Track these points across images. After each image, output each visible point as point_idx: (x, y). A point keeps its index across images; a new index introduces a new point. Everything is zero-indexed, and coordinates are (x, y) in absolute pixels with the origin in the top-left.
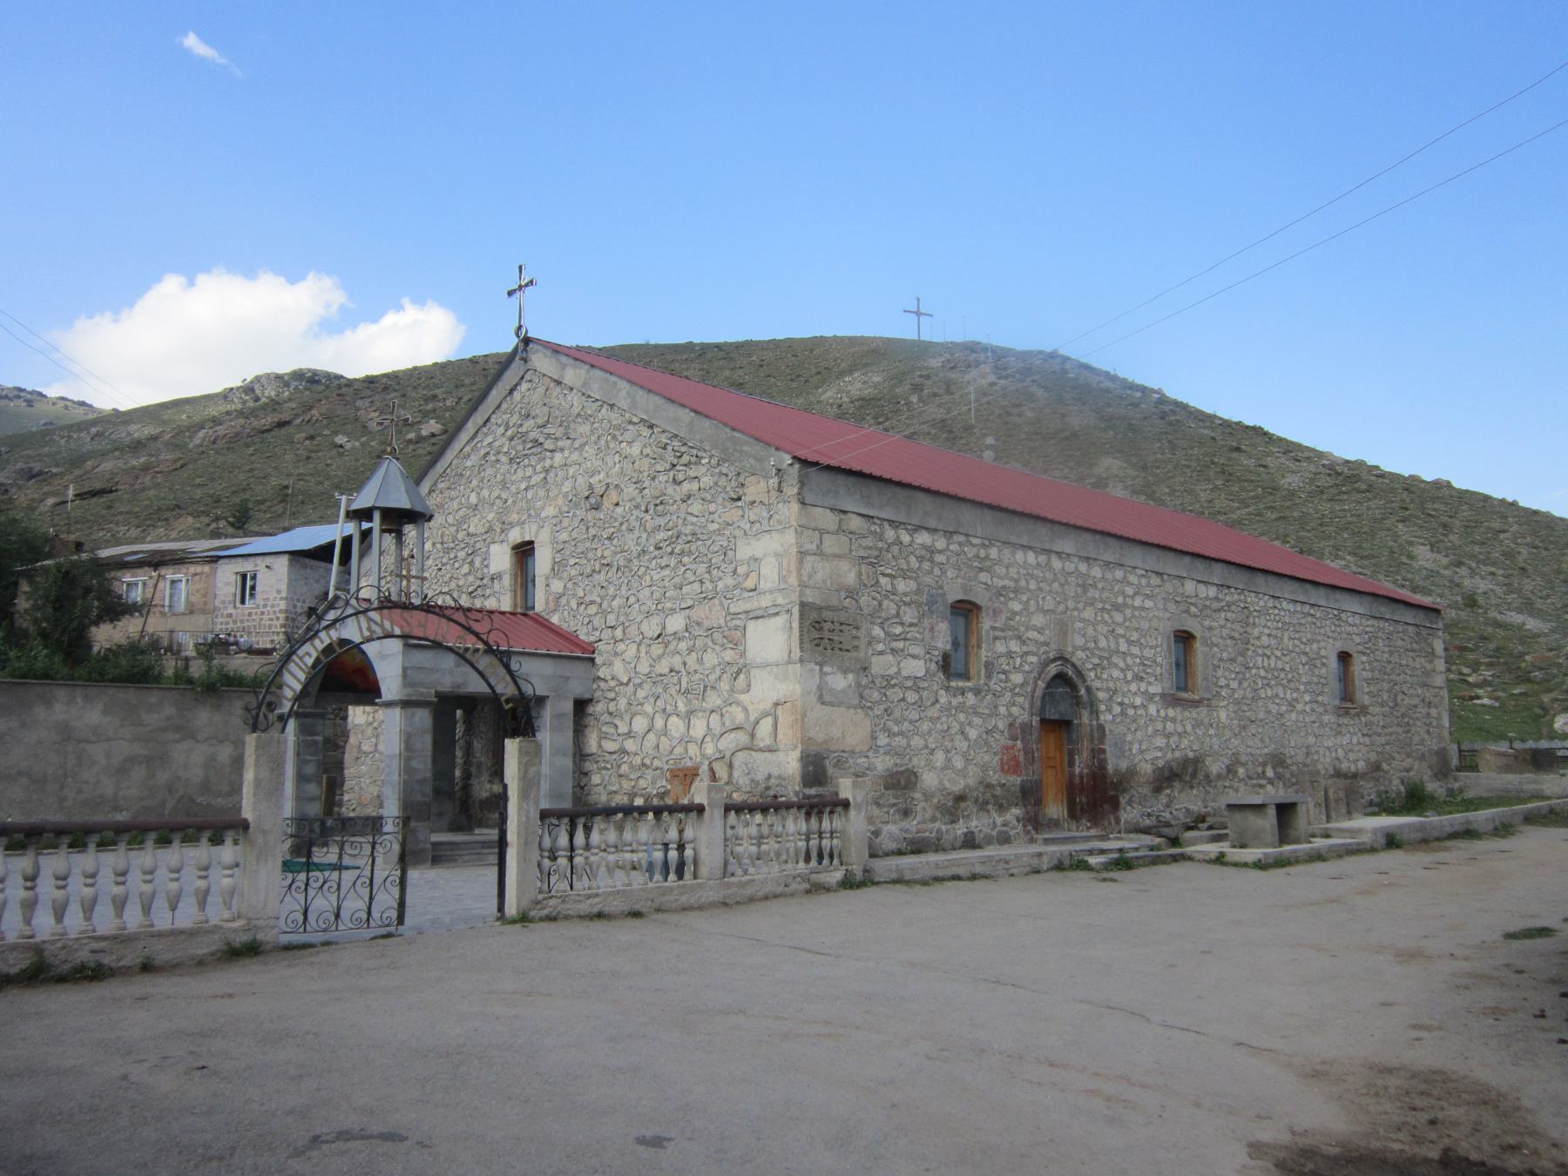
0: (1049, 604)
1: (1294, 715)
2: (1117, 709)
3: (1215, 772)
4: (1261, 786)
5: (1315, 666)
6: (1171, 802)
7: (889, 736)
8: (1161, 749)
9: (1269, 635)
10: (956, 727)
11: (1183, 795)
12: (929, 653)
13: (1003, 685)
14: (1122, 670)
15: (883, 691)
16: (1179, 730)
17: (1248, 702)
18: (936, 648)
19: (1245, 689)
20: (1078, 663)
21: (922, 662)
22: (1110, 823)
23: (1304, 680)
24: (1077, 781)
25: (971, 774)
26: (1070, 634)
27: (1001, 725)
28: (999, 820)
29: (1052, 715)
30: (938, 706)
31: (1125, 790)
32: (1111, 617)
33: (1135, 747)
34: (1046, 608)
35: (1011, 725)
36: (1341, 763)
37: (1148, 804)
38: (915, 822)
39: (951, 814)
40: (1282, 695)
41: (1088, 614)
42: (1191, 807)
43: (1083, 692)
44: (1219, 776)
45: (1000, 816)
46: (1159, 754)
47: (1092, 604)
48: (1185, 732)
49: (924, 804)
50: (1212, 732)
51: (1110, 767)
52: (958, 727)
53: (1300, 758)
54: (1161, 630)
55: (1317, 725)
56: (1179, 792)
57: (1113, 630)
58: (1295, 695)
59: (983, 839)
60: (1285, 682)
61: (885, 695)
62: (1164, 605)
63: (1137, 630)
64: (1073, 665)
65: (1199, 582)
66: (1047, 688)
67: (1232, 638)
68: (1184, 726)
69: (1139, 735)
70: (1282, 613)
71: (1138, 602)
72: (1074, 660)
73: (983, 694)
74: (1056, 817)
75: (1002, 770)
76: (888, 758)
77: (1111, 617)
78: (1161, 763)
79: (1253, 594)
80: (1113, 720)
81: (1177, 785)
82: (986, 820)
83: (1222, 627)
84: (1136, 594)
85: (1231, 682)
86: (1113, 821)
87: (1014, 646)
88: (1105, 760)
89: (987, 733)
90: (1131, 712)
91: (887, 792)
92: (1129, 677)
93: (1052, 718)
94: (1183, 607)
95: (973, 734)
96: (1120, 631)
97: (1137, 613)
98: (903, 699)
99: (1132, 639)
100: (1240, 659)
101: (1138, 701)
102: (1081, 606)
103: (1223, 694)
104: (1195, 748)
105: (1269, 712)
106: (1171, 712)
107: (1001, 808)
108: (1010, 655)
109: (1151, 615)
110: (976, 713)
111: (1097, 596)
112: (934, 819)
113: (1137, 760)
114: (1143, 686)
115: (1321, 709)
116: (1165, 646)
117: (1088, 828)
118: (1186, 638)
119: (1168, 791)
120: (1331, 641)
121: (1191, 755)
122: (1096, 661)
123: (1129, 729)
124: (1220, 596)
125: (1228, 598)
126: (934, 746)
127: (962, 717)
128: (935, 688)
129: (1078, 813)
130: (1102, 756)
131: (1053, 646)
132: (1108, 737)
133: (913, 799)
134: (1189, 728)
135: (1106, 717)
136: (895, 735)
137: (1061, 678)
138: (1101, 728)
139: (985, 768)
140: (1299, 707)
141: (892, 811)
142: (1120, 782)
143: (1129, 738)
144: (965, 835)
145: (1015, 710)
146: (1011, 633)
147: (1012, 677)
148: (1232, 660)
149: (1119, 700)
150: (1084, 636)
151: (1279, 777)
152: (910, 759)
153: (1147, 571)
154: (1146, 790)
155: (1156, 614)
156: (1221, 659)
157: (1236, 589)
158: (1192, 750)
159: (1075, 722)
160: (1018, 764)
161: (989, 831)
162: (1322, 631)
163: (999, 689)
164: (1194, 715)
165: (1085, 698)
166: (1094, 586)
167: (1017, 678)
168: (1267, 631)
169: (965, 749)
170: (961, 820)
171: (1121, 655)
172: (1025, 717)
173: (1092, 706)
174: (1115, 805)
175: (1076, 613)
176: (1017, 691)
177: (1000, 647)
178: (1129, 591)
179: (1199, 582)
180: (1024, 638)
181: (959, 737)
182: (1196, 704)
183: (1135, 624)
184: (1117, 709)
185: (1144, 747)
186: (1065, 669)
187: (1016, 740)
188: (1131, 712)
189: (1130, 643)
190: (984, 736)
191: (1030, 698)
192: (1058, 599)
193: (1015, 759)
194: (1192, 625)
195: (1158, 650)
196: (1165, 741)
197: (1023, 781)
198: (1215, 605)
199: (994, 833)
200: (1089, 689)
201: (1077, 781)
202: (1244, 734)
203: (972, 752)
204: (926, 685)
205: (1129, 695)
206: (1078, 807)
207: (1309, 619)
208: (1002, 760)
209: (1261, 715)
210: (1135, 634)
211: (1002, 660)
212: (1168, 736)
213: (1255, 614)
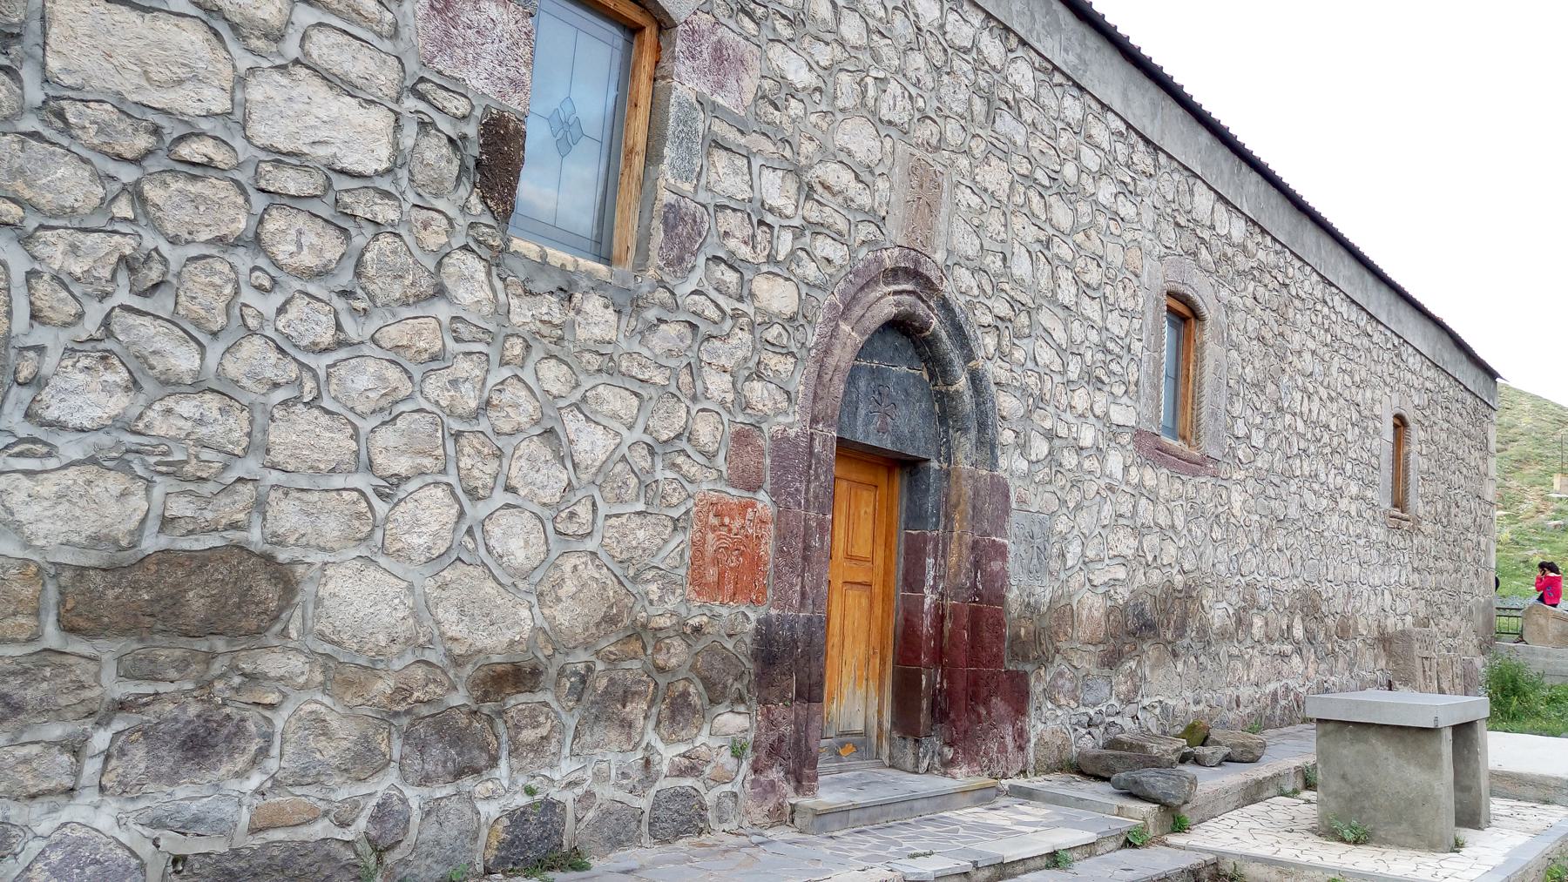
0: (894, 106)
1: (1336, 518)
2: (1040, 448)
3: (1217, 623)
4: (1283, 656)
5: (1365, 429)
6: (1136, 690)
7: (134, 385)
8: (1124, 561)
9: (1313, 352)
10: (519, 408)
11: (1161, 672)
12: (422, 97)
13: (722, 300)
14: (1060, 351)
15: (128, 174)
16: (1161, 521)
17: (1276, 480)
18: (455, 87)
19: (1273, 453)
20: (958, 302)
21: (379, 120)
22: (1003, 749)
23: (1352, 454)
24: (926, 625)
25: (569, 587)
26: (944, 211)
27: (705, 431)
28: (668, 754)
29: (868, 433)
30: (442, 311)
31: (1043, 661)
32: (1047, 207)
33: (1074, 549)
34: (886, 114)
35: (742, 438)
36: (1386, 617)
37: (1090, 698)
38: (255, 780)
39: (458, 738)
40: (1323, 477)
41: (995, 176)
42: (1171, 702)
43: (962, 383)
44: (1224, 635)
45: (667, 742)
46: (1121, 573)
47: (1005, 156)
48: (1173, 527)
49: (320, 703)
50: (1217, 533)
51: (1013, 595)
52: (529, 407)
53: (1338, 604)
54: (1145, 278)
55: (1362, 542)
56: (1153, 668)
57: (1047, 244)
58: (1339, 480)
59: (596, 826)
60: (1328, 450)
61: (136, 195)
62: (1156, 223)
63: (1098, 259)
64: (945, 305)
65: (1221, 197)
66: (864, 352)
67: (1261, 339)
68: (1171, 513)
69: (1085, 520)
70: (1333, 317)
71: (1106, 191)
72: (947, 288)
73: (651, 315)
74: (859, 727)
75: (698, 582)
76: (114, 483)
77: (1047, 207)
78: (1122, 595)
79: (1298, 264)
80: (1028, 475)
81: (1150, 650)
82: (613, 756)
83: (1248, 311)
84: (1102, 173)
85: (1253, 431)
86: (1009, 741)
87: (775, 190)
88: (1004, 575)
89: (652, 452)
90: (1069, 460)
91: (80, 646)
92: (1074, 371)
93: (873, 442)
94: (1189, 242)
95: (591, 444)
96: (1065, 252)
97: (1102, 220)
98: (255, 242)
99: (1087, 278)
100: (1271, 388)
101: (1087, 437)
102: (979, 148)
103: (1240, 454)
104: (1187, 567)
105: (1303, 506)
106: (1150, 478)
107: (678, 712)
108: (760, 217)
109: (1128, 236)
110: (610, 369)
111: (1020, 140)
112: (365, 761)
113: (1074, 583)
114: (1101, 402)
115: (1368, 514)
116: (1149, 317)
117: (948, 764)
118: (1184, 319)
119: (1133, 664)
120: (1388, 390)
121: (1179, 580)
122: (1002, 309)
123: (1063, 502)
124: (1250, 245)
125: (1261, 255)
126: (402, 465)
127: (553, 376)
128: (434, 239)
129: (924, 718)
130: (996, 566)
131: (895, 233)
132: (1015, 517)
133: (252, 678)
134: (1179, 522)
135: (1011, 464)
136: (171, 384)
137: (902, 327)
138: (1000, 489)
139: (631, 569)
140: (1344, 504)
141: (101, 739)
142: (1036, 637)
143: (1062, 525)
144: (517, 818)
145: (757, 391)
146: (768, 147)
147: (761, 285)
148: (1258, 386)
149: (1048, 424)
150: (978, 230)
151: (1311, 638)
152: (260, 505)
153: (1129, 126)
154: (1087, 662)
155: (1138, 235)
156: (1242, 379)
157: (1274, 239)
158: (1183, 572)
159: (934, 464)
160: (756, 562)
161: (620, 795)
162: (1379, 368)
163: (712, 312)
164: (1191, 492)
165: (968, 403)
166: (1014, 107)
167: (778, 296)
168: (1311, 345)
169: (551, 494)
170: (503, 764)
171: (1058, 311)
172: (792, 422)
173: (982, 427)
174: (1019, 698)
175: (963, 162)
176: (773, 333)
177: (726, 177)
178: (1091, 159)
179: (1221, 197)
180: (808, 177)
181: (534, 447)
182: (1197, 465)
183: (1094, 245)
184: (1040, 448)
185: (1091, 554)
186: (921, 310)
187: (754, 488)
188: (1069, 460)
189: (1085, 288)
190: (640, 459)
191: (813, 368)
192: (921, 103)
193: (746, 548)
194: (1202, 291)
195: (1136, 324)
196: (1133, 543)
197: (766, 622)
198: (1242, 262)
199: (644, 803)
200: (976, 379)
201: (926, 625)
202: (1265, 546)
203: (584, 511)
204: (386, 212)
205: (1068, 416)
206: (925, 704)
207: (1365, 341)
208: (698, 547)
209: (1293, 512)
210: (1093, 266)
211: (730, 221)
212: (1139, 532)
213: (1297, 303)
